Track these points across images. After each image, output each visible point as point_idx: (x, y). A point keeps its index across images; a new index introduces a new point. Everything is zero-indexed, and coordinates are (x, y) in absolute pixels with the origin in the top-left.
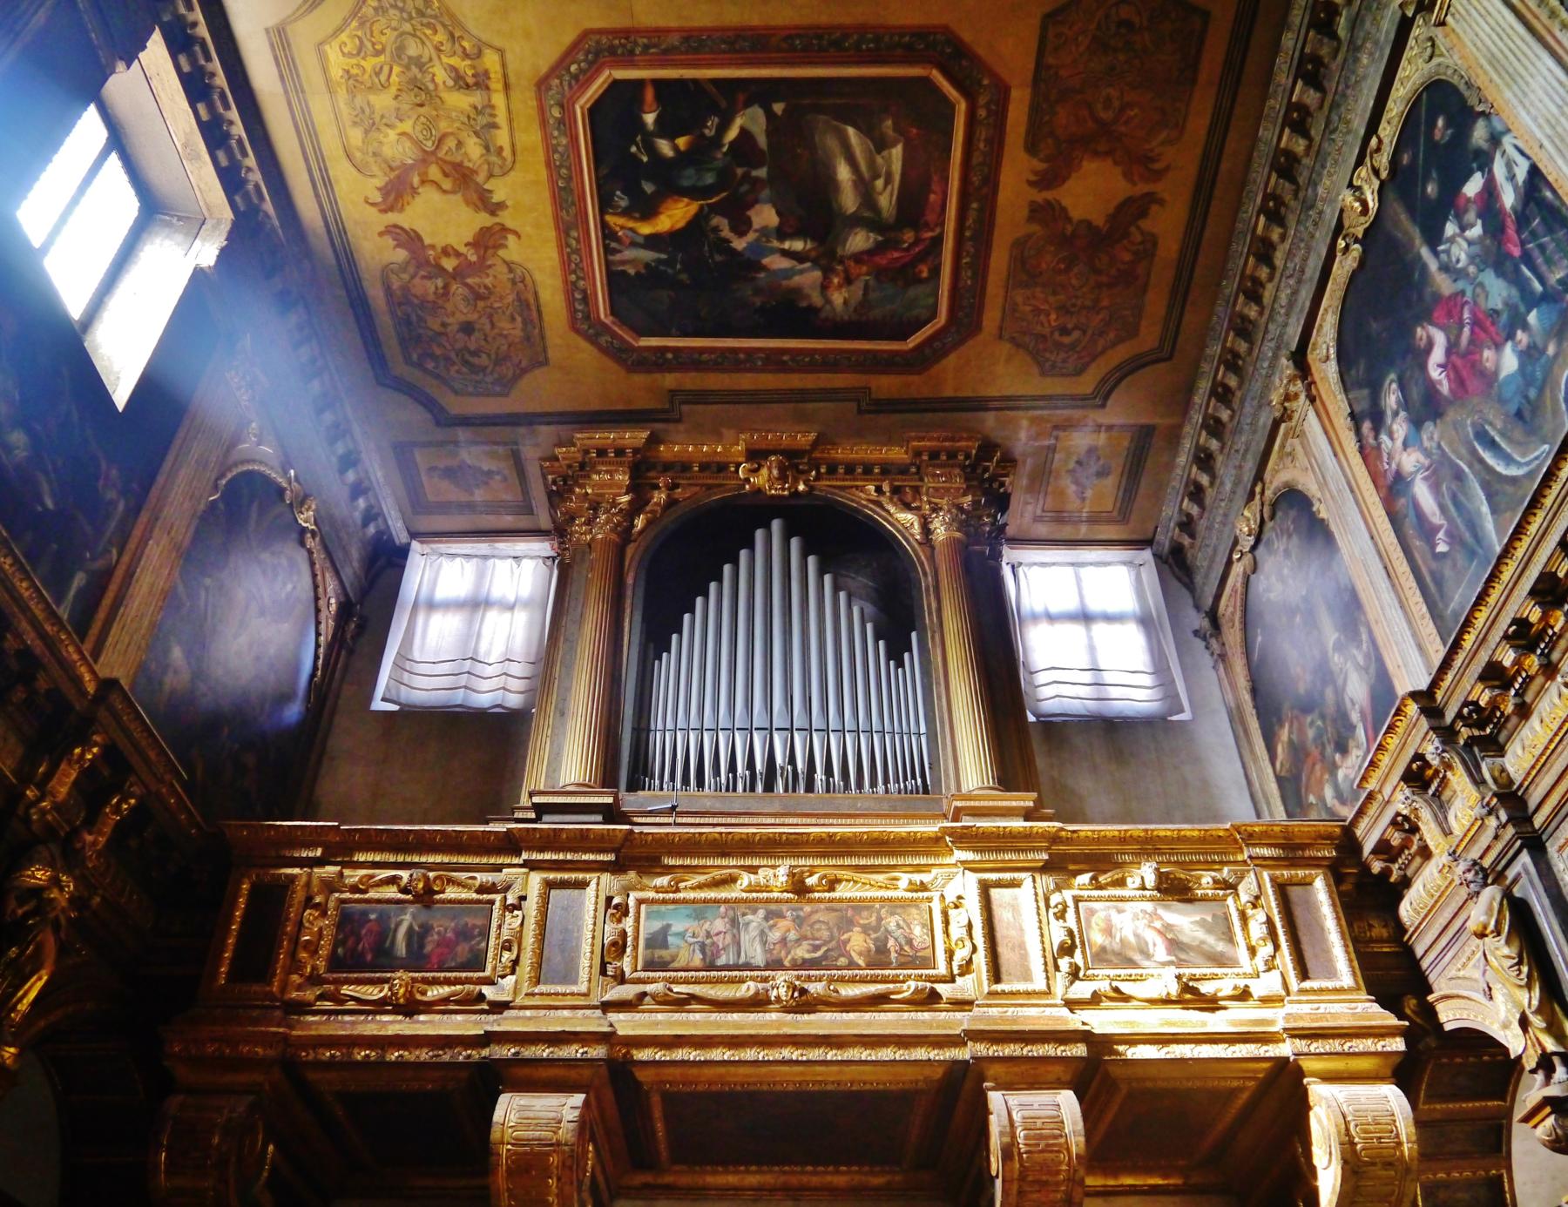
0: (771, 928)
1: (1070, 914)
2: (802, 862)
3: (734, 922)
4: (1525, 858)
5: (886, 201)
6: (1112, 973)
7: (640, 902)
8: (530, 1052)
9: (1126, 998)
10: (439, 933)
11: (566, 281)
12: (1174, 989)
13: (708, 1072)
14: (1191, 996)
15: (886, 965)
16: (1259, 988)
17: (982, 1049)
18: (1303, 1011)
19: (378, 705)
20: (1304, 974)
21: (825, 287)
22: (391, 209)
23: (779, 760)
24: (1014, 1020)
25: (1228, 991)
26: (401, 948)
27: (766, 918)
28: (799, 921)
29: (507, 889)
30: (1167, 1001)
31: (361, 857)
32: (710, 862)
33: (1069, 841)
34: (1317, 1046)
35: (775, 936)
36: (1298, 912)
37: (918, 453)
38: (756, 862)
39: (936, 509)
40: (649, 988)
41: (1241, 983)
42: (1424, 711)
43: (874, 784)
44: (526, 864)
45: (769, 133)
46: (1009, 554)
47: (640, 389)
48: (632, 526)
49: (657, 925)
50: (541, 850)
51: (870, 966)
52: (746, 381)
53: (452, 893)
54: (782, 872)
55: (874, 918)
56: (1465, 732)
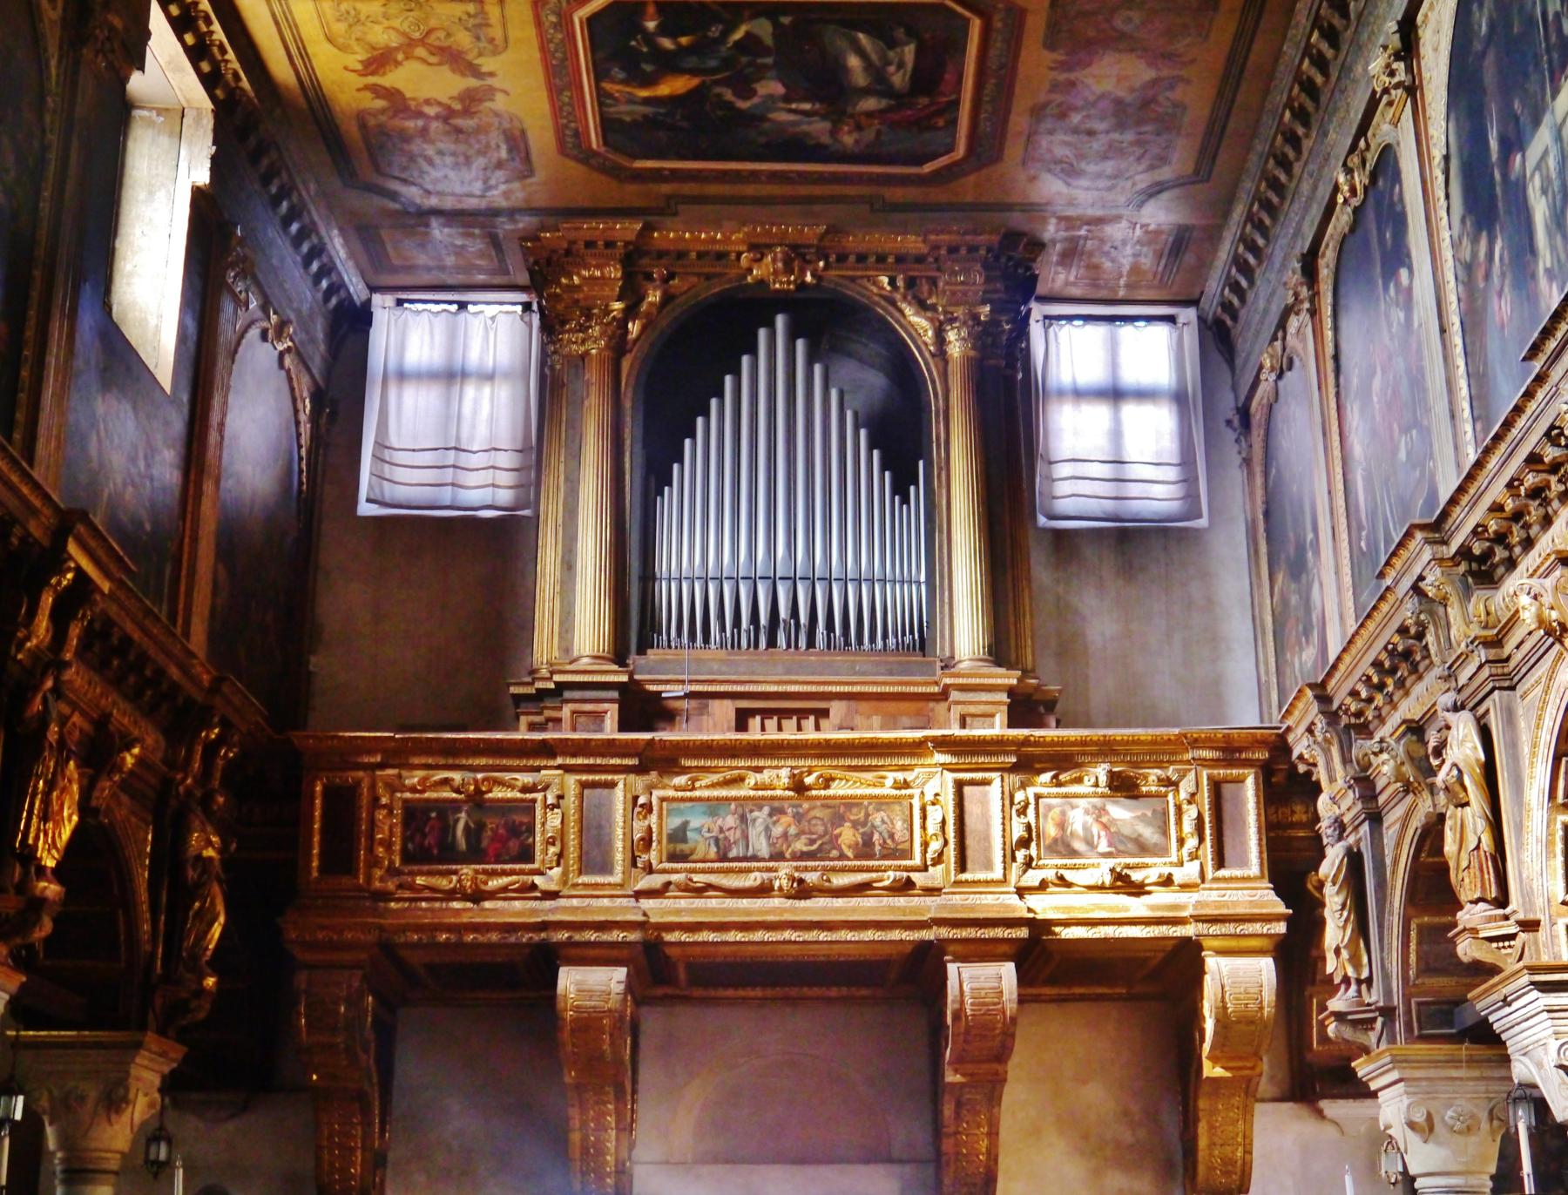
0: (775, 823)
1: (1031, 811)
2: (801, 763)
3: (743, 819)
4: (1366, 827)
5: (898, 79)
6: (1060, 862)
7: (663, 800)
8: (577, 937)
9: (1068, 885)
10: (492, 829)
11: (556, 123)
12: (1108, 880)
13: (727, 949)
14: (1124, 884)
15: (871, 857)
16: (1179, 876)
17: (944, 933)
18: (1212, 898)
19: (365, 509)
20: (1220, 862)
21: (834, 133)
22: (373, 73)
23: (783, 613)
24: (972, 908)
25: (1153, 878)
26: (462, 843)
27: (770, 815)
28: (798, 817)
29: (545, 789)
30: (1101, 888)
31: (416, 760)
32: (721, 763)
33: (1037, 744)
34: (1215, 929)
35: (777, 831)
36: (1227, 807)
37: (936, 247)
38: (761, 763)
39: (952, 320)
40: (674, 878)
41: (1166, 871)
42: (1316, 697)
43: (873, 639)
44: (559, 767)
45: (774, 35)
46: (1037, 310)
47: (632, 194)
48: (626, 331)
49: (674, 822)
50: (574, 755)
51: (857, 857)
52: (750, 190)
53: (498, 793)
54: (785, 773)
55: (862, 814)
56: (1344, 720)
